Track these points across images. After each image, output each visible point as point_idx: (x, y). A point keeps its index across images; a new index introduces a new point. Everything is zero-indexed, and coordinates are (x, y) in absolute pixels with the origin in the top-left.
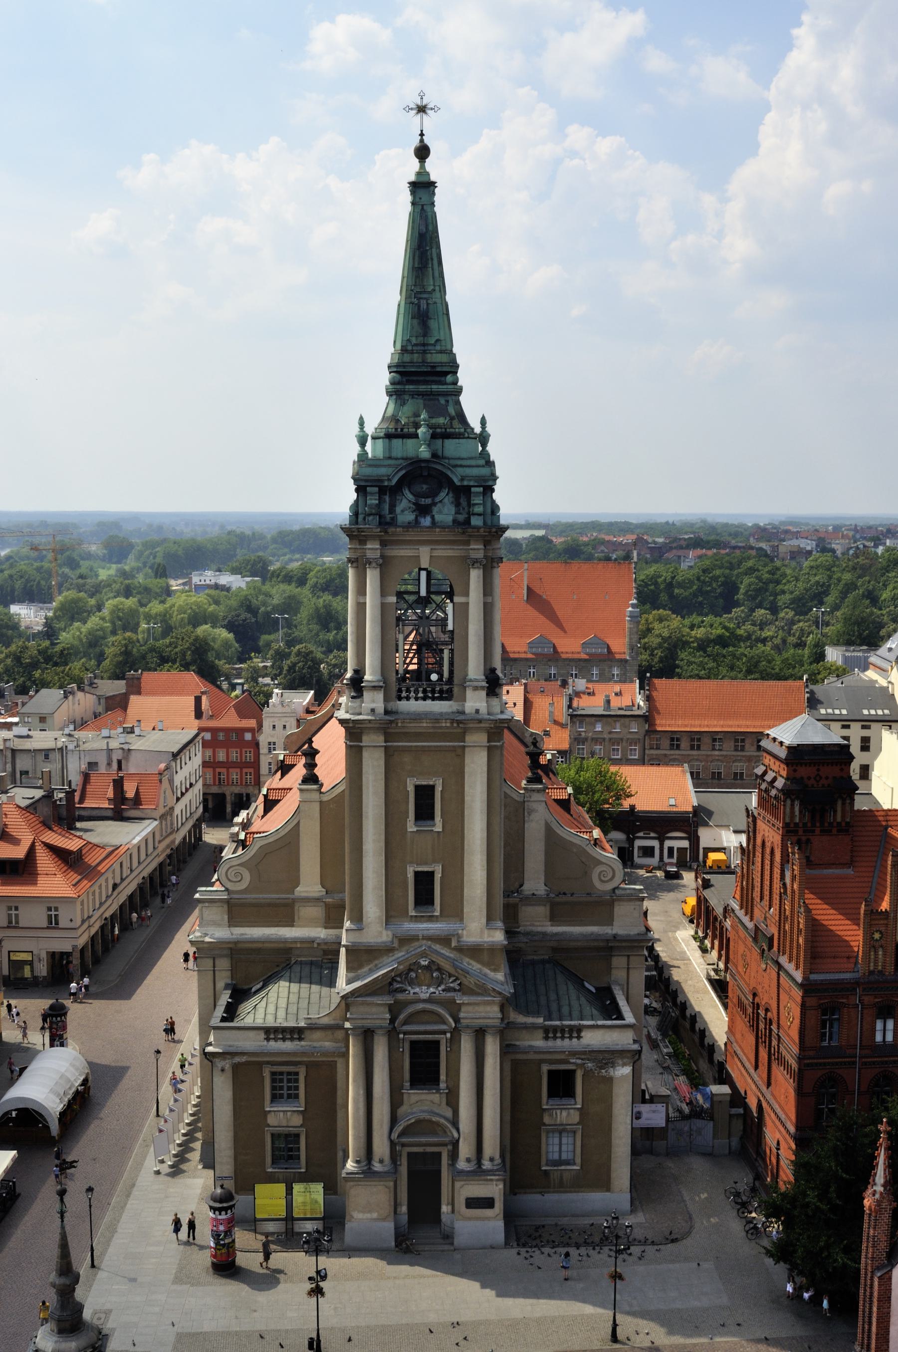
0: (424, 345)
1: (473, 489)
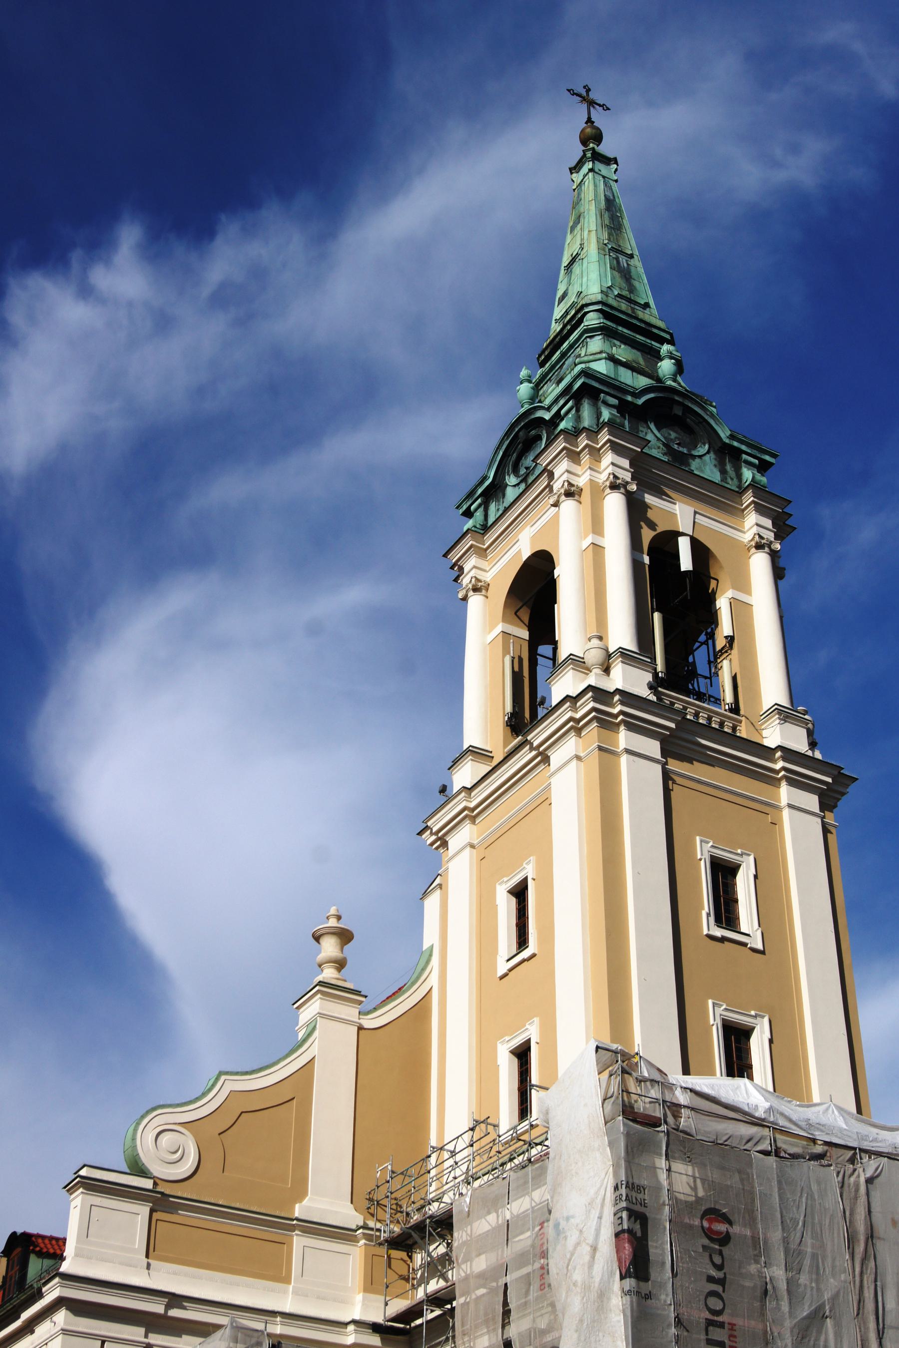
0: (630, 301)
1: (744, 456)
